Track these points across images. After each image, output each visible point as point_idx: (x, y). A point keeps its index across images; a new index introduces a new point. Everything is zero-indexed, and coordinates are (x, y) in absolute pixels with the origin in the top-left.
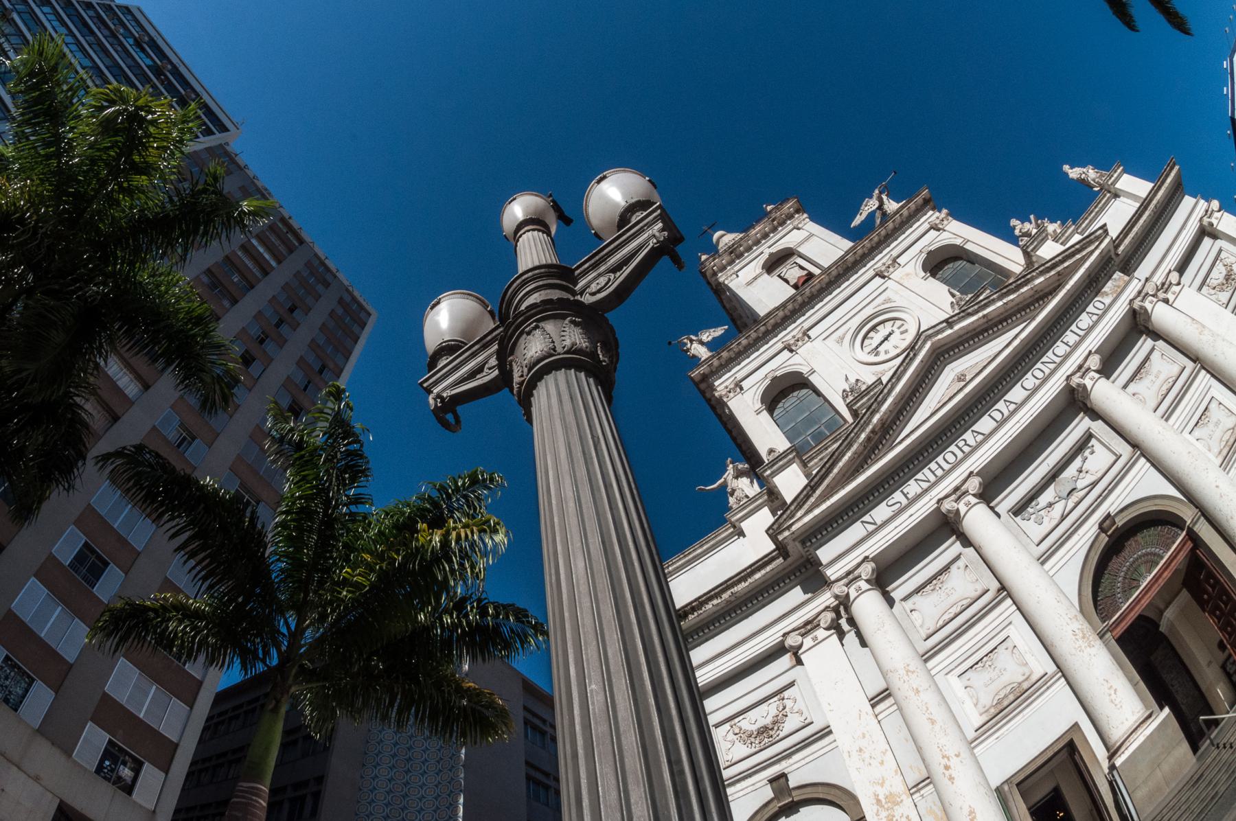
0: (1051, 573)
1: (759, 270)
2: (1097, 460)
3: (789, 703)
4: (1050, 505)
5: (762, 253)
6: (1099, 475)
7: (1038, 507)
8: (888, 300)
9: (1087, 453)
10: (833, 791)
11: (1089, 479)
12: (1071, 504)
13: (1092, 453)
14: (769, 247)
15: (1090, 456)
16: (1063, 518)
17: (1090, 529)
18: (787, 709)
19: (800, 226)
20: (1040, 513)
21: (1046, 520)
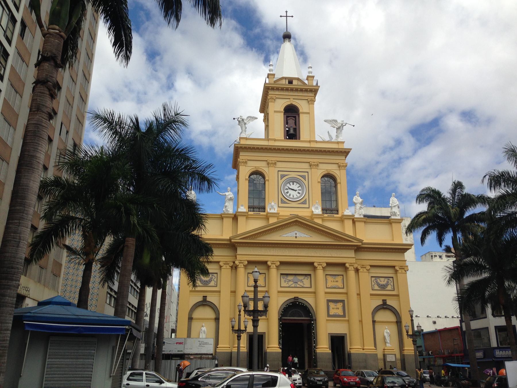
0: (279, 296)
1: (282, 110)
2: (306, 282)
3: (214, 277)
4: (290, 280)
5: (290, 99)
6: (305, 286)
7: (287, 278)
8: (303, 177)
9: (306, 278)
10: (215, 307)
11: (302, 284)
12: (293, 286)
13: (307, 279)
14: (293, 99)
15: (306, 279)
16: (289, 287)
17: (292, 296)
18: (213, 279)
19: (310, 102)
20: (287, 280)
21: (287, 282)
